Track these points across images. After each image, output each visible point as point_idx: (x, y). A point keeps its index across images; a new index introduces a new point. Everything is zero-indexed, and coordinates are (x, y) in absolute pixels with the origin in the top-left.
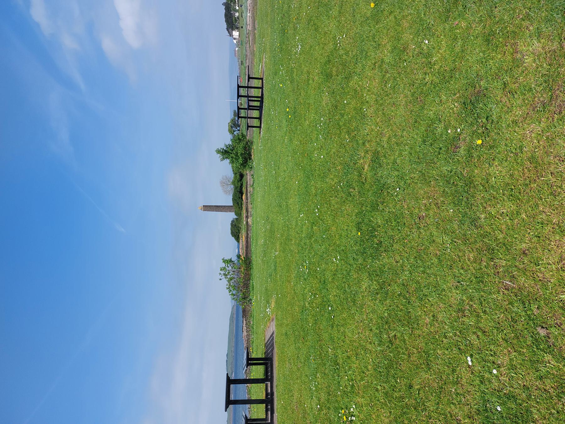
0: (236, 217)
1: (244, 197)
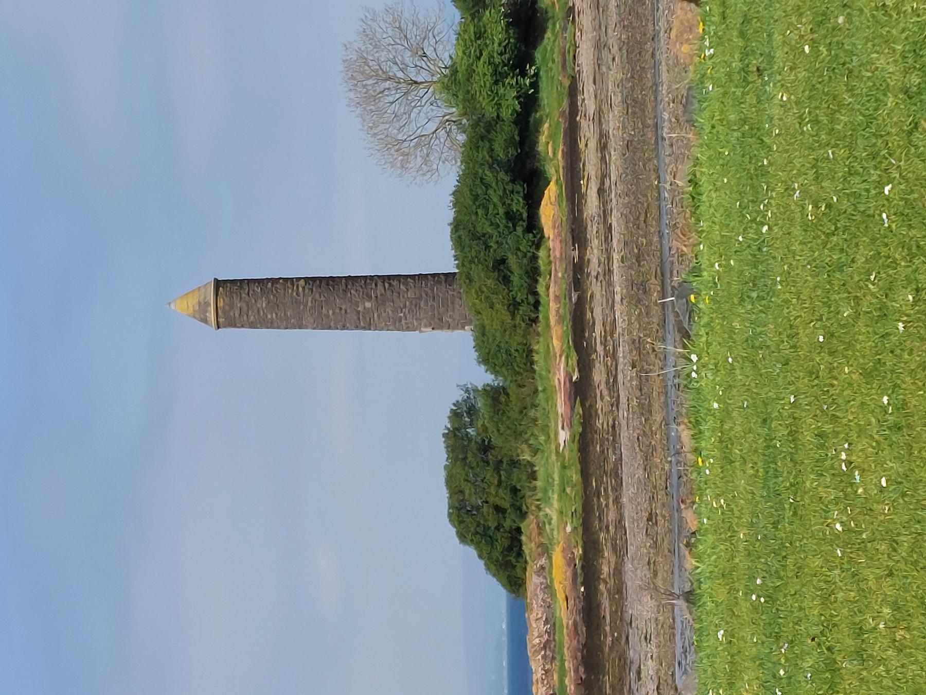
0: (483, 377)
1: (550, 211)
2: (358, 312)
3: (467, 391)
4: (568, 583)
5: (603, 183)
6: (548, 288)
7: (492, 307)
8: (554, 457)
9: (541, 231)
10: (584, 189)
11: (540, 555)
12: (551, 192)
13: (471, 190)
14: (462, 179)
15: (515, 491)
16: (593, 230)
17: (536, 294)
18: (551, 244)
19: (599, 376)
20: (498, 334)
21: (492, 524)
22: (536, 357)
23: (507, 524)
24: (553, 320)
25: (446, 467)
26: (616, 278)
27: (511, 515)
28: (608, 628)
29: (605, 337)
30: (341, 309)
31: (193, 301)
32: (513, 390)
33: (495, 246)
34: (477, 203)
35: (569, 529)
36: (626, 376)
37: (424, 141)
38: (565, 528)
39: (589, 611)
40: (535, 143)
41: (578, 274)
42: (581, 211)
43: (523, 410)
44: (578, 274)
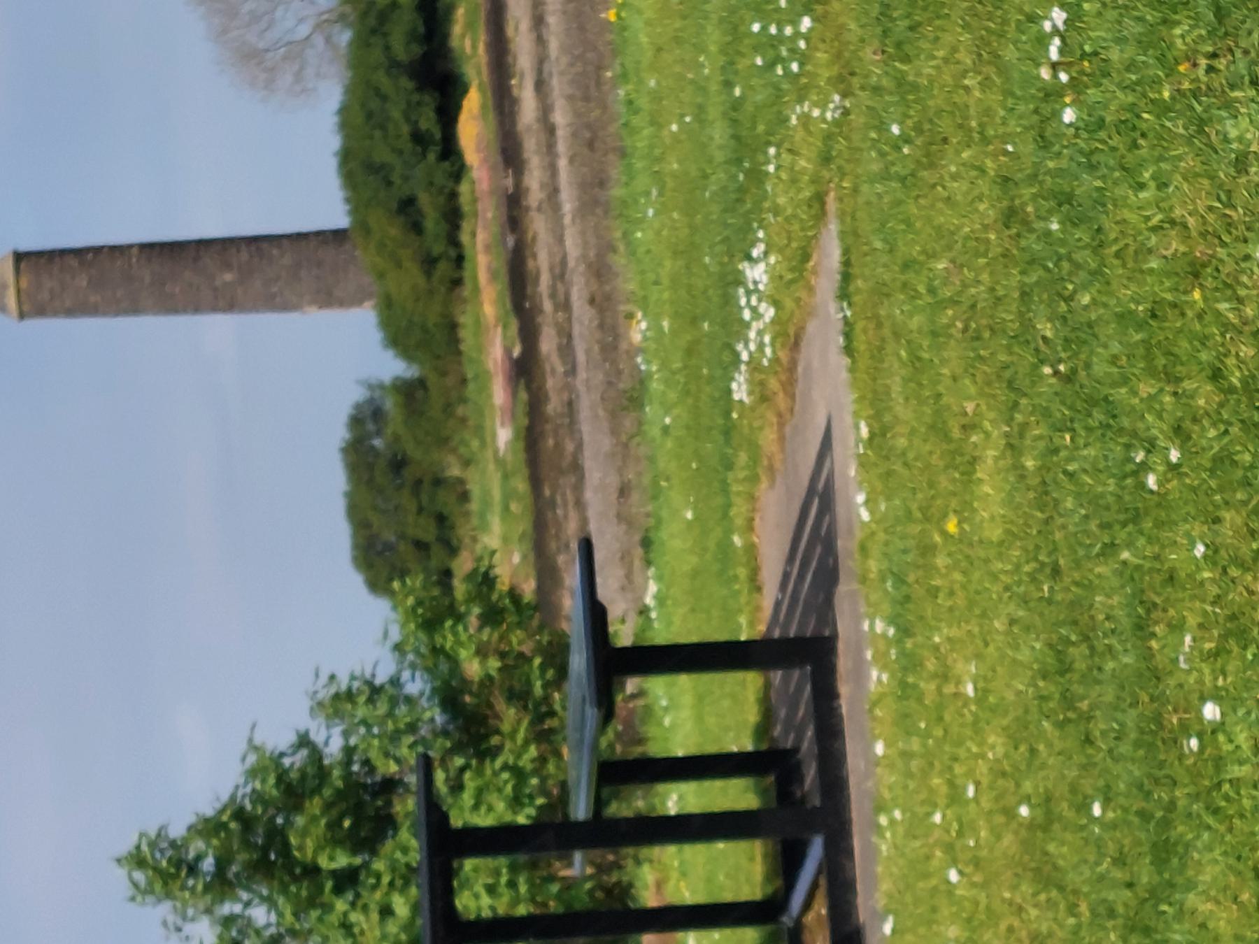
1: (472, 128)
2: (215, 289)
3: (371, 387)
6: (474, 235)
8: (491, 467)
10: (515, 92)
12: (473, 104)
13: (363, 105)
14: (349, 91)
15: (441, 519)
19: (548, 344)
24: (483, 277)
27: (437, 551)
32: (432, 379)
35: (516, 559)
37: (296, 50)
38: (510, 560)
40: (446, 36)
41: (514, 208)
42: (513, 123)
43: (448, 409)
44: (514, 208)
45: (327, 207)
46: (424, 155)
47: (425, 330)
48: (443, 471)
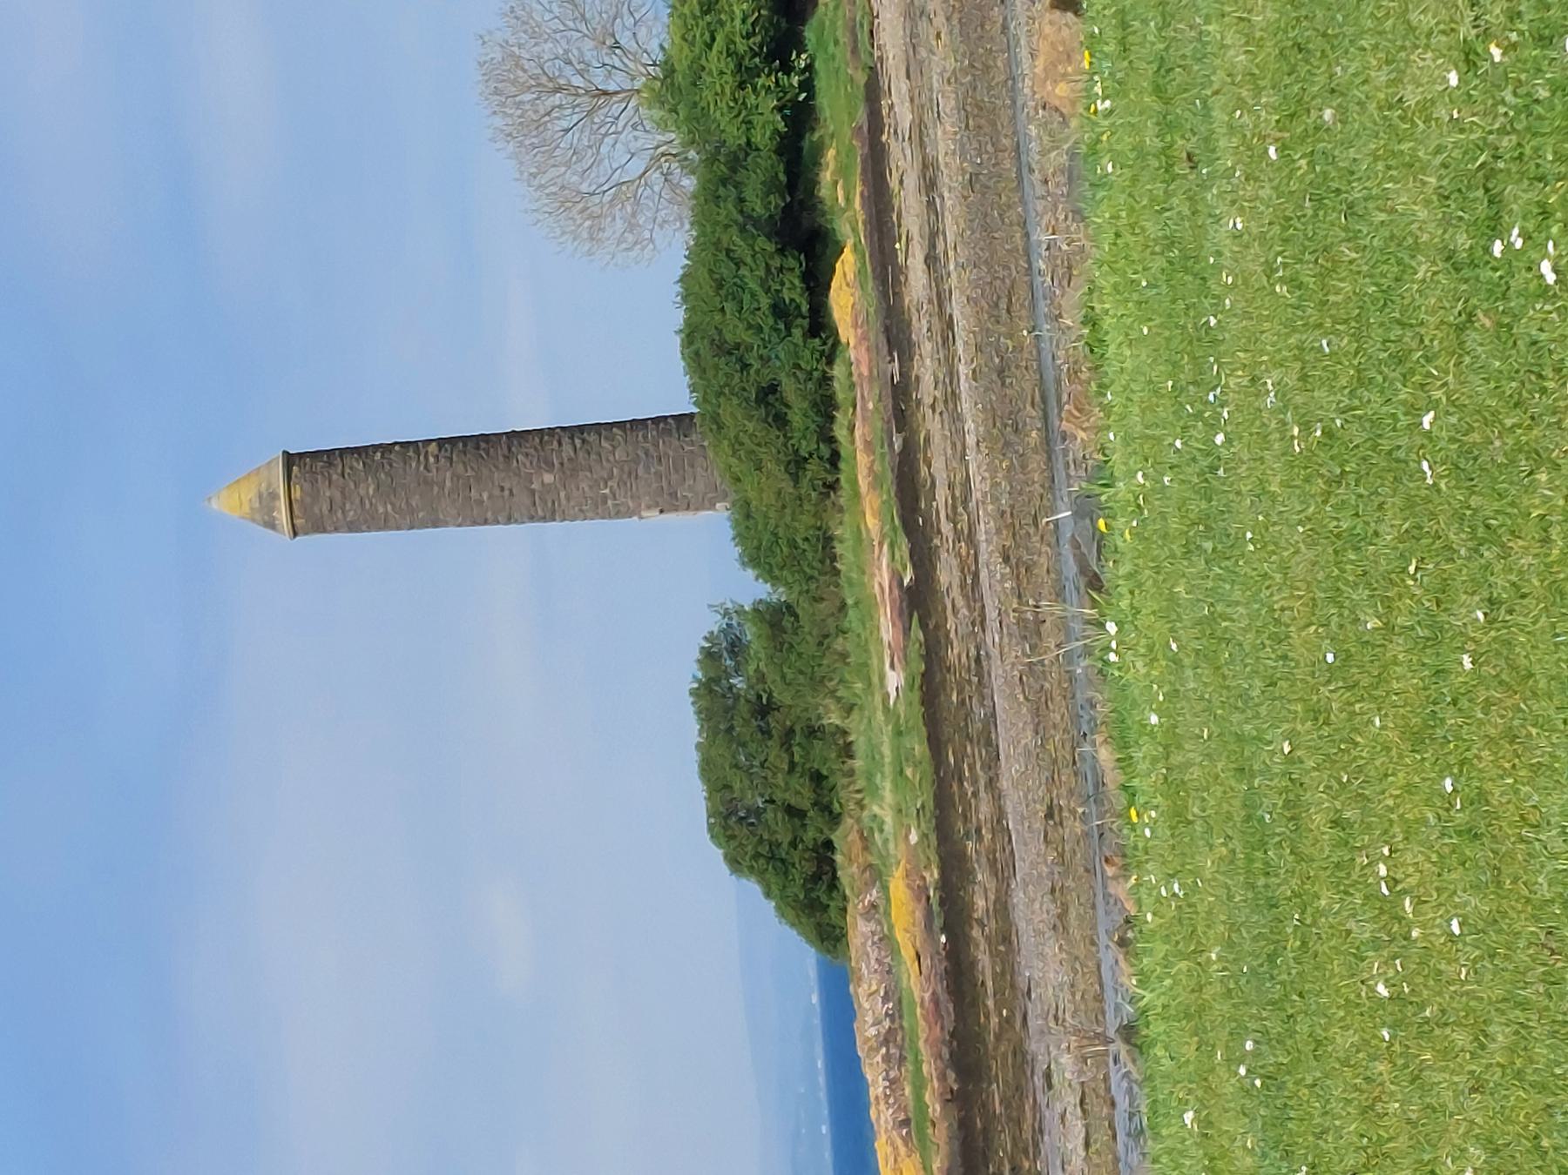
0: (752, 589)
1: (846, 298)
2: (533, 492)
3: (726, 613)
4: (919, 931)
5: (933, 246)
6: (852, 429)
7: (759, 469)
8: (880, 716)
9: (835, 333)
10: (901, 258)
11: (869, 885)
12: (847, 266)
13: (711, 271)
15: (818, 778)
16: (921, 327)
17: (831, 440)
18: (852, 354)
19: (947, 574)
20: (772, 514)
21: (784, 838)
22: (839, 549)
23: (810, 835)
25: (698, 746)
26: (966, 406)
28: (990, 1003)
29: (954, 507)
30: (502, 489)
31: (248, 494)
32: (804, 608)
33: (756, 365)
34: (723, 292)
35: (914, 838)
36: (993, 572)
37: (625, 191)
38: (907, 837)
39: (957, 975)
40: (814, 183)
42: (898, 295)
44: (901, 402)
45: (667, 388)
46: (788, 328)
47: (793, 545)
48: (819, 717)
